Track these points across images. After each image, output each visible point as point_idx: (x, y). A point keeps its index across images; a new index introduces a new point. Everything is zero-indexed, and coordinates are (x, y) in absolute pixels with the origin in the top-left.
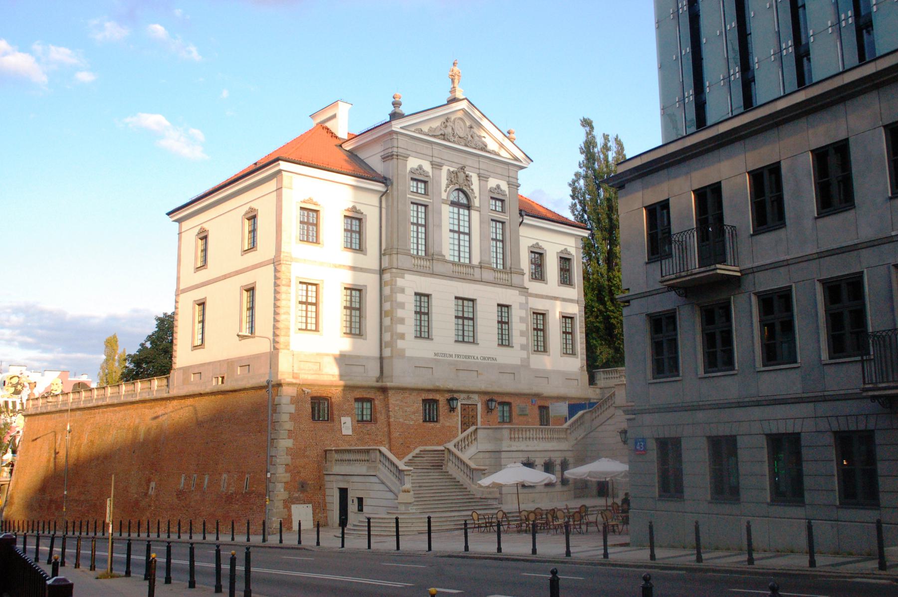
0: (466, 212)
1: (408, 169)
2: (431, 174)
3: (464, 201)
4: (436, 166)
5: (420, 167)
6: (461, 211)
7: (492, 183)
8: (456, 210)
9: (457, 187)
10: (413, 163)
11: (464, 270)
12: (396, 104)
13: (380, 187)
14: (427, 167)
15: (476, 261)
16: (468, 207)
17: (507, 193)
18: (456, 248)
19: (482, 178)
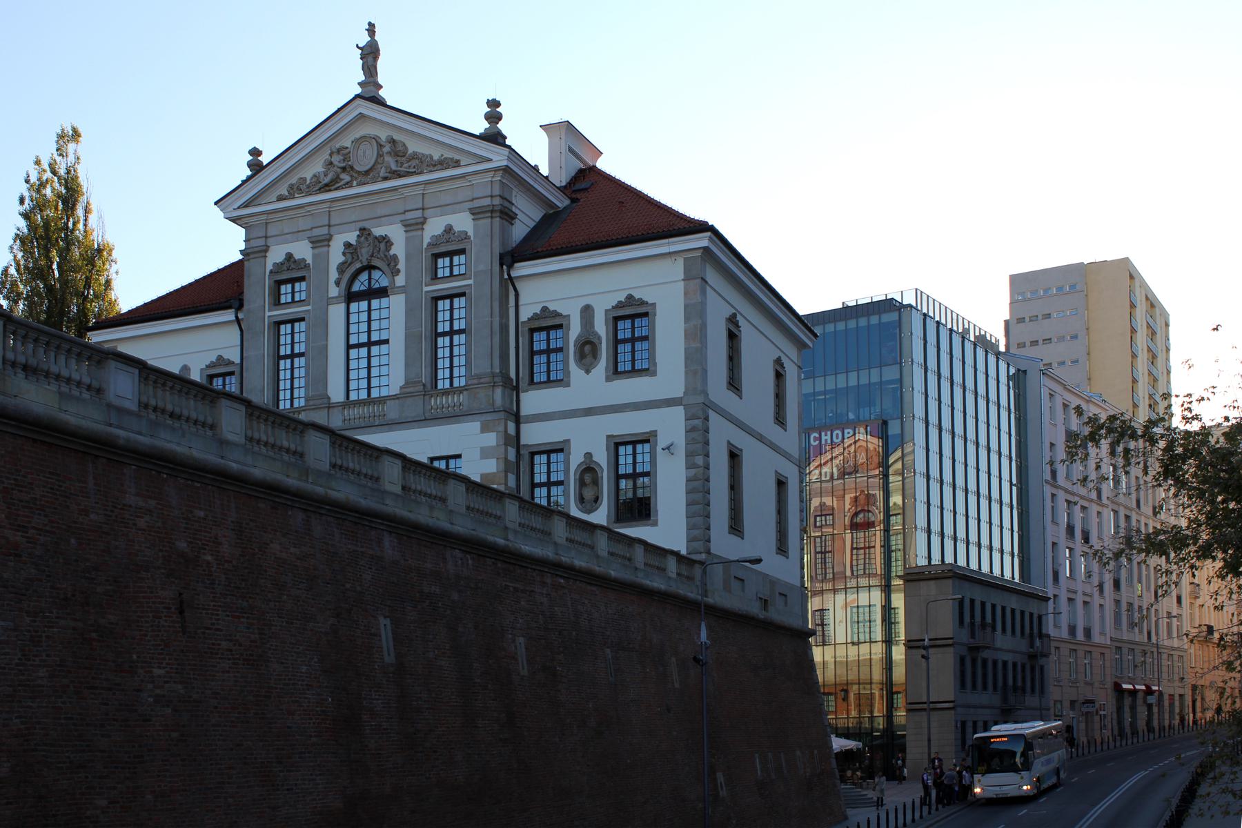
0: (384, 301)
1: (269, 267)
2: (309, 261)
3: (384, 282)
4: (321, 242)
5: (289, 256)
6: (375, 303)
7: (435, 227)
8: (364, 305)
9: (358, 265)
10: (276, 255)
11: (366, 411)
12: (256, 167)
13: (229, 315)
14: (302, 250)
15: (395, 390)
16: (383, 292)
17: (471, 233)
18: (374, 372)
19: (414, 226)
